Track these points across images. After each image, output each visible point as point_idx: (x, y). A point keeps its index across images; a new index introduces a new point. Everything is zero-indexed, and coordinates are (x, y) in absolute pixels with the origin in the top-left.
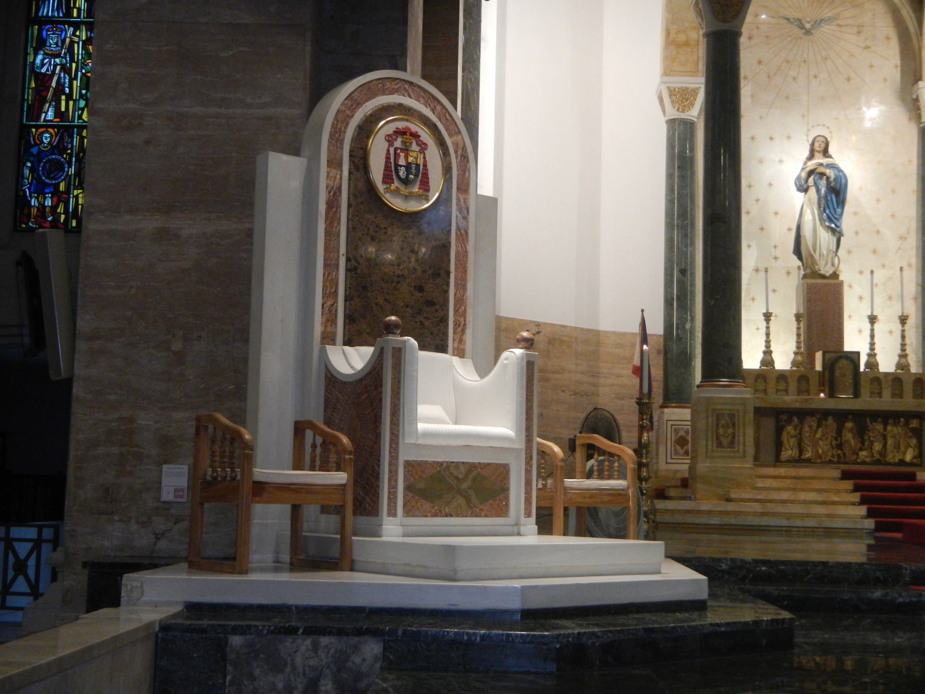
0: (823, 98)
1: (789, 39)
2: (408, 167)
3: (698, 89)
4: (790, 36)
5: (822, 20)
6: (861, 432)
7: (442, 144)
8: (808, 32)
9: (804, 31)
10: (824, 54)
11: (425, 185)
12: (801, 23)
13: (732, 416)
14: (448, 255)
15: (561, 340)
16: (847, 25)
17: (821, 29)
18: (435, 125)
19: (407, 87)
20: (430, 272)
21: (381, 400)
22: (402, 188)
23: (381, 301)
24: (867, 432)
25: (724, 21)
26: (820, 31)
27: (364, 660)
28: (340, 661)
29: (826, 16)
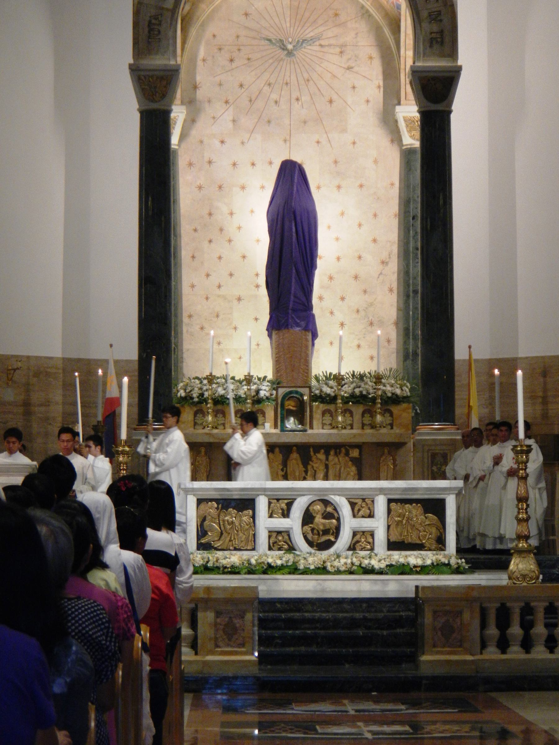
0: (305, 122)
1: (271, 61)
4: (272, 58)
5: (304, 41)
6: (306, 460)
8: (290, 54)
9: (286, 52)
10: (306, 76)
12: (283, 44)
15: (46, 372)
16: (330, 45)
17: (303, 49)
24: (310, 463)
25: (153, 101)
26: (301, 52)
29: (309, 36)
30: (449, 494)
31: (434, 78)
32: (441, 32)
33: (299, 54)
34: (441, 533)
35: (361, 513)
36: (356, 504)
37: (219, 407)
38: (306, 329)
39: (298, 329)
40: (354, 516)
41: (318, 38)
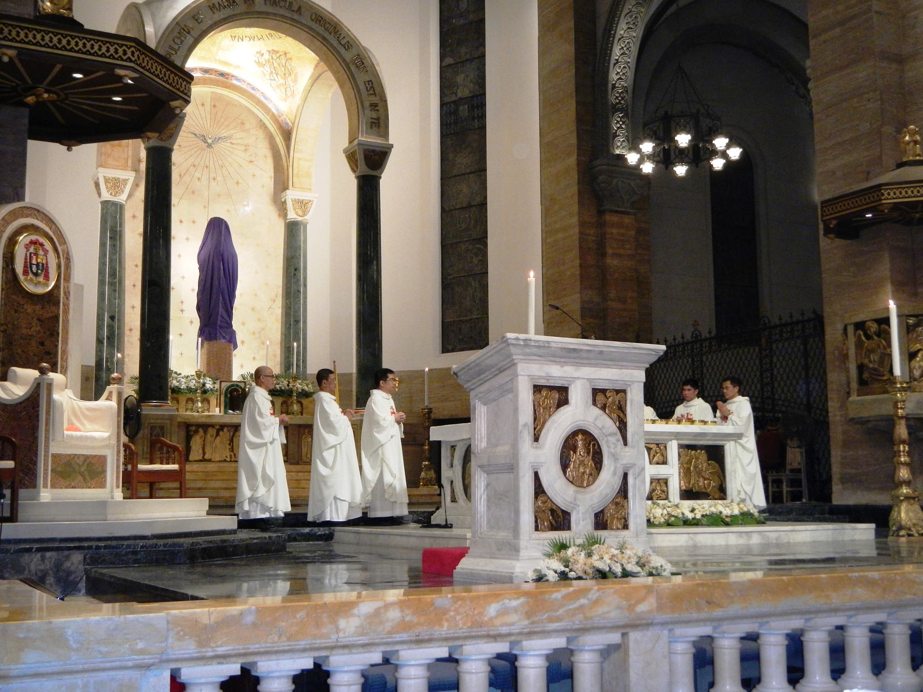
0: (219, 196)
2: (37, 265)
3: (127, 180)
7: (56, 249)
8: (209, 146)
11: (47, 277)
13: (162, 428)
14: (58, 322)
16: (238, 144)
18: (52, 239)
19: (36, 213)
20: (48, 333)
21: (38, 416)
22: (34, 278)
23: (19, 351)
25: (162, 140)
27: (72, 564)
28: (58, 566)
30: (729, 441)
31: (373, 151)
32: (378, 119)
33: (216, 147)
34: (722, 481)
35: (656, 459)
36: (651, 449)
37: (175, 395)
38: (230, 341)
39: (224, 341)
40: (651, 463)
41: (230, 137)
